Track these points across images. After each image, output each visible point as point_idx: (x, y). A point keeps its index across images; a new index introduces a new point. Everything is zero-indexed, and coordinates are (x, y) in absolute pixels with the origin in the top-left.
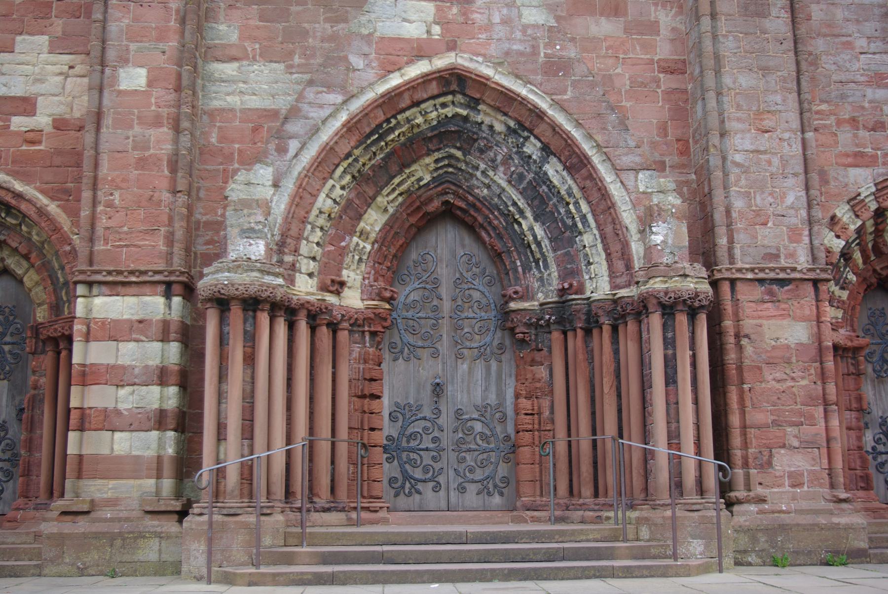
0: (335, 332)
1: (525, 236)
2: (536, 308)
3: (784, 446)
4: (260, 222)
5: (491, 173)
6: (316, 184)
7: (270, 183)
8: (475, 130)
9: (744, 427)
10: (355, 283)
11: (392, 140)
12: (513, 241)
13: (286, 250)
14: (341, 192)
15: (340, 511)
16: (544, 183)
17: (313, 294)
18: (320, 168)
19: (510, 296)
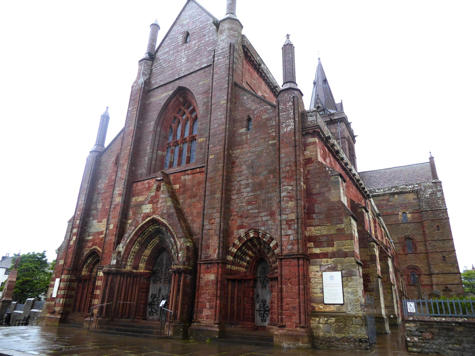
3: (205, 308)
9: (198, 302)
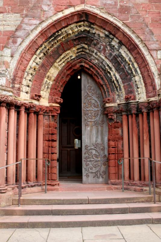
0: (38, 116)
1: (112, 78)
2: (117, 106)
4: (4, 70)
5: (99, 54)
6: (28, 56)
7: (10, 55)
8: (92, 36)
10: (46, 96)
11: (60, 40)
12: (107, 80)
13: (16, 82)
14: (40, 60)
15: (39, 186)
16: (120, 57)
17: (27, 100)
18: (30, 50)
19: (106, 102)
